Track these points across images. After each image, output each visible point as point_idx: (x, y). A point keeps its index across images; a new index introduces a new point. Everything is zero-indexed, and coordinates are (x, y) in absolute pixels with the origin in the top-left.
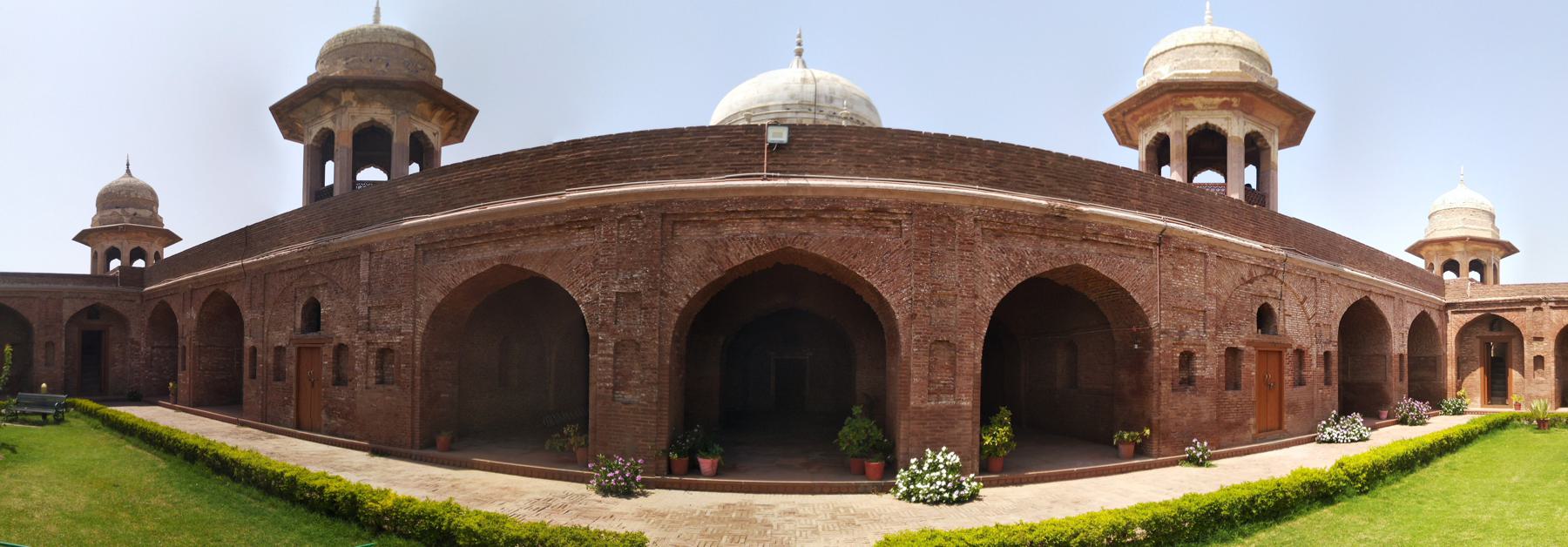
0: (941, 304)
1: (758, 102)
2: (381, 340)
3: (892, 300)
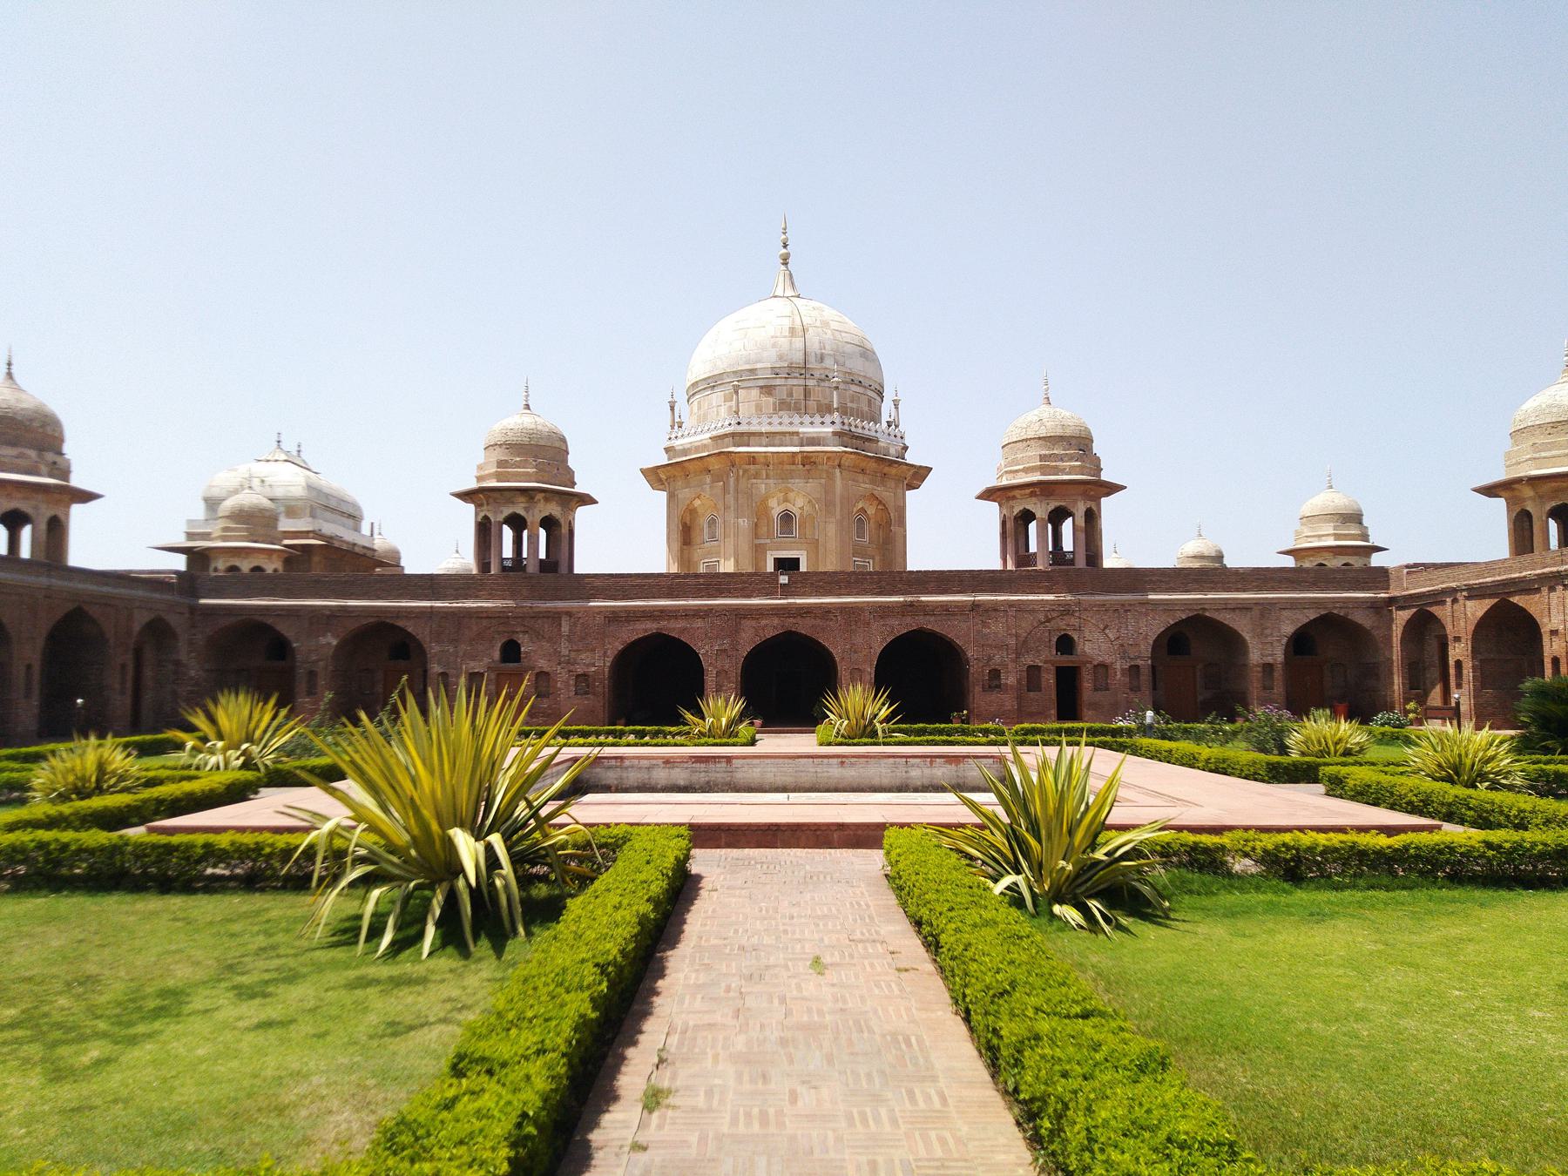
0: (855, 652)
2: (580, 671)
3: (834, 652)
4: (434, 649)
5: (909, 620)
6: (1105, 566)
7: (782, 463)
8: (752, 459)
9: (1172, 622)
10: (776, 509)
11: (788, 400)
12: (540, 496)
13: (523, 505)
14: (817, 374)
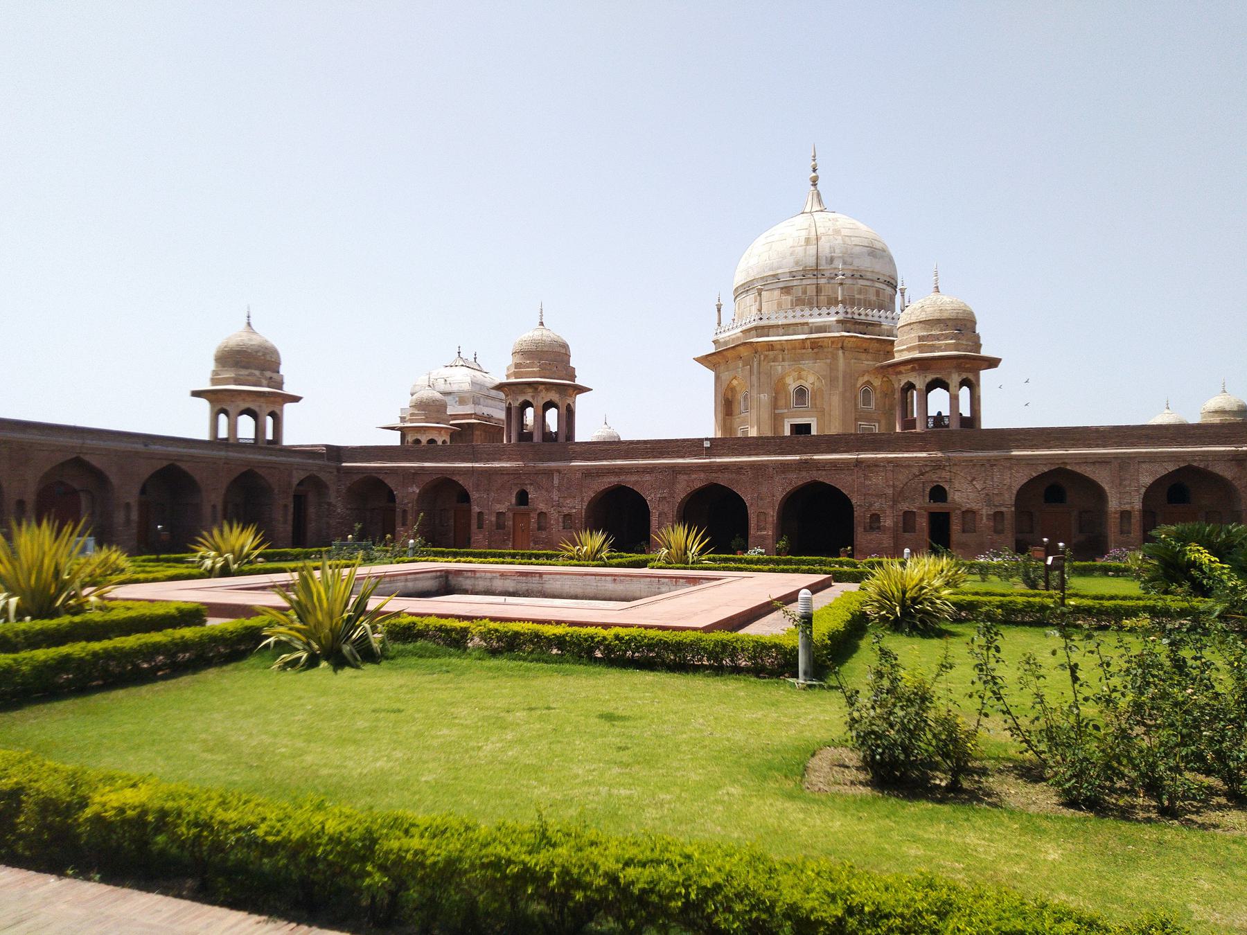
1: (770, 270)
2: (566, 511)
4: (474, 495)
5: (804, 474)
6: (982, 428)
7: (794, 348)
8: (771, 346)
9: (1035, 475)
10: (792, 385)
12: (541, 387)
13: (531, 394)
14: (827, 274)
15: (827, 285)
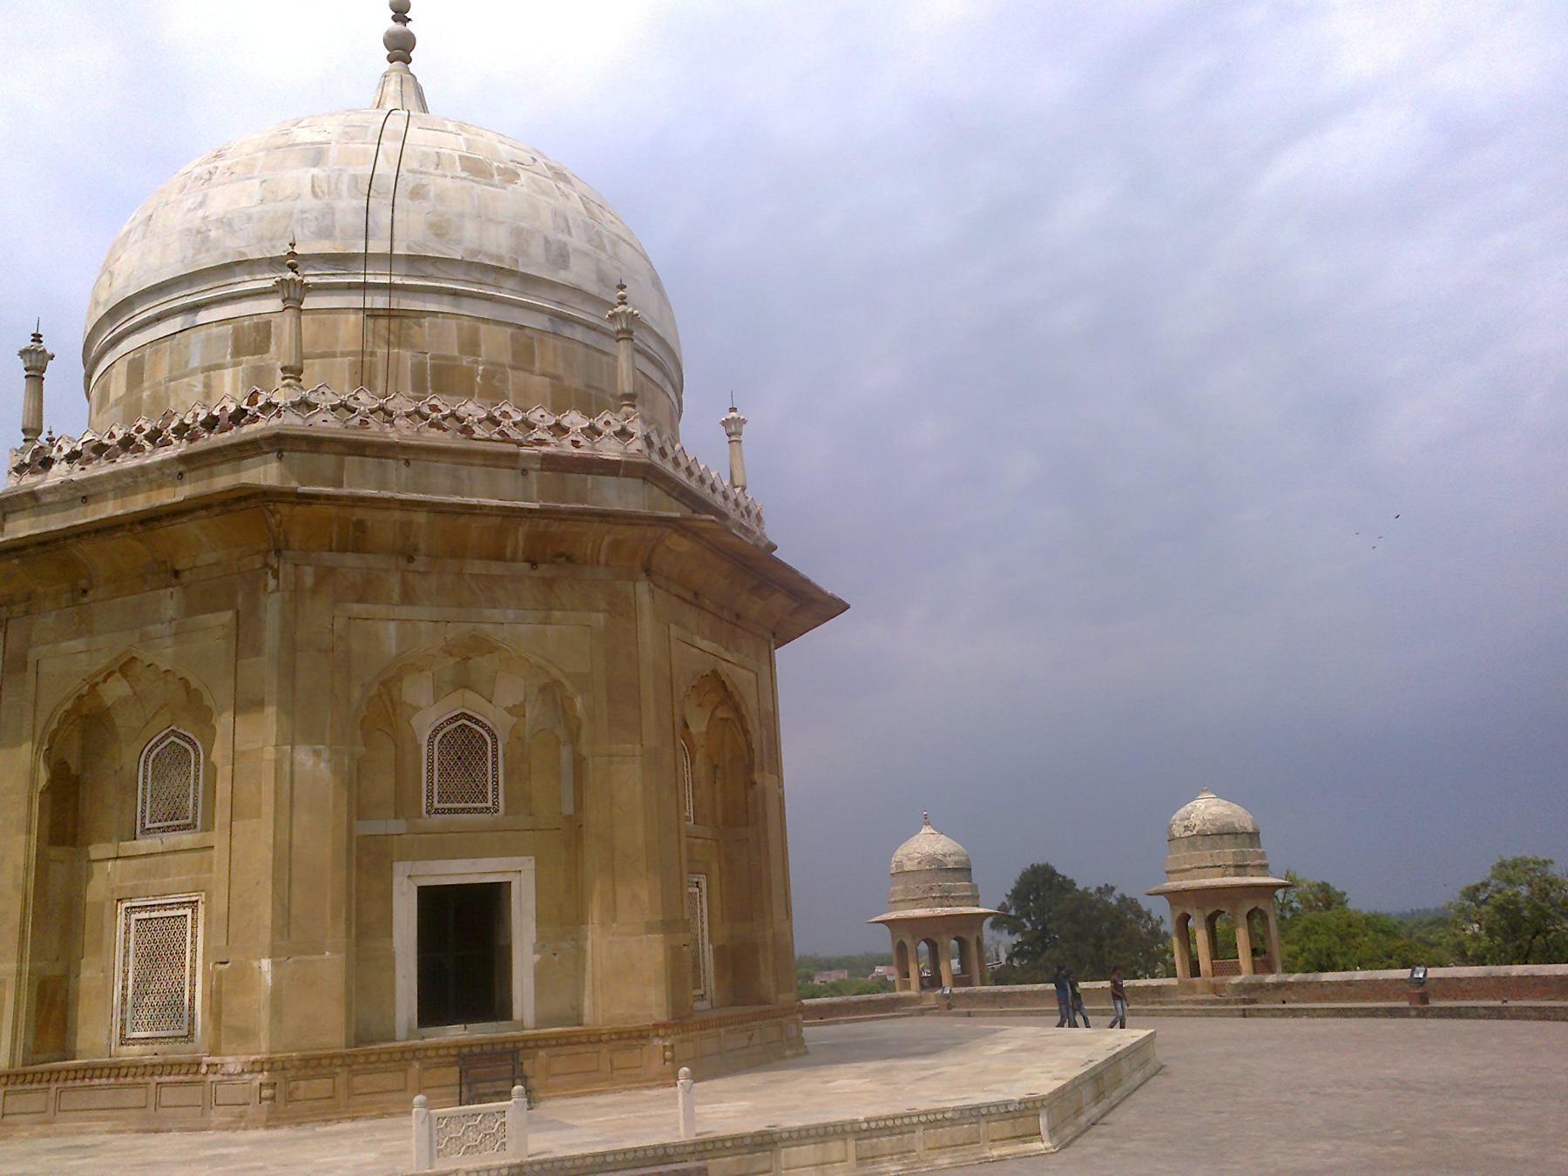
11: (466, 361)
15: (549, 340)
